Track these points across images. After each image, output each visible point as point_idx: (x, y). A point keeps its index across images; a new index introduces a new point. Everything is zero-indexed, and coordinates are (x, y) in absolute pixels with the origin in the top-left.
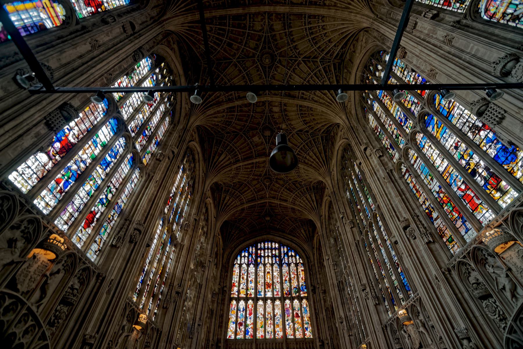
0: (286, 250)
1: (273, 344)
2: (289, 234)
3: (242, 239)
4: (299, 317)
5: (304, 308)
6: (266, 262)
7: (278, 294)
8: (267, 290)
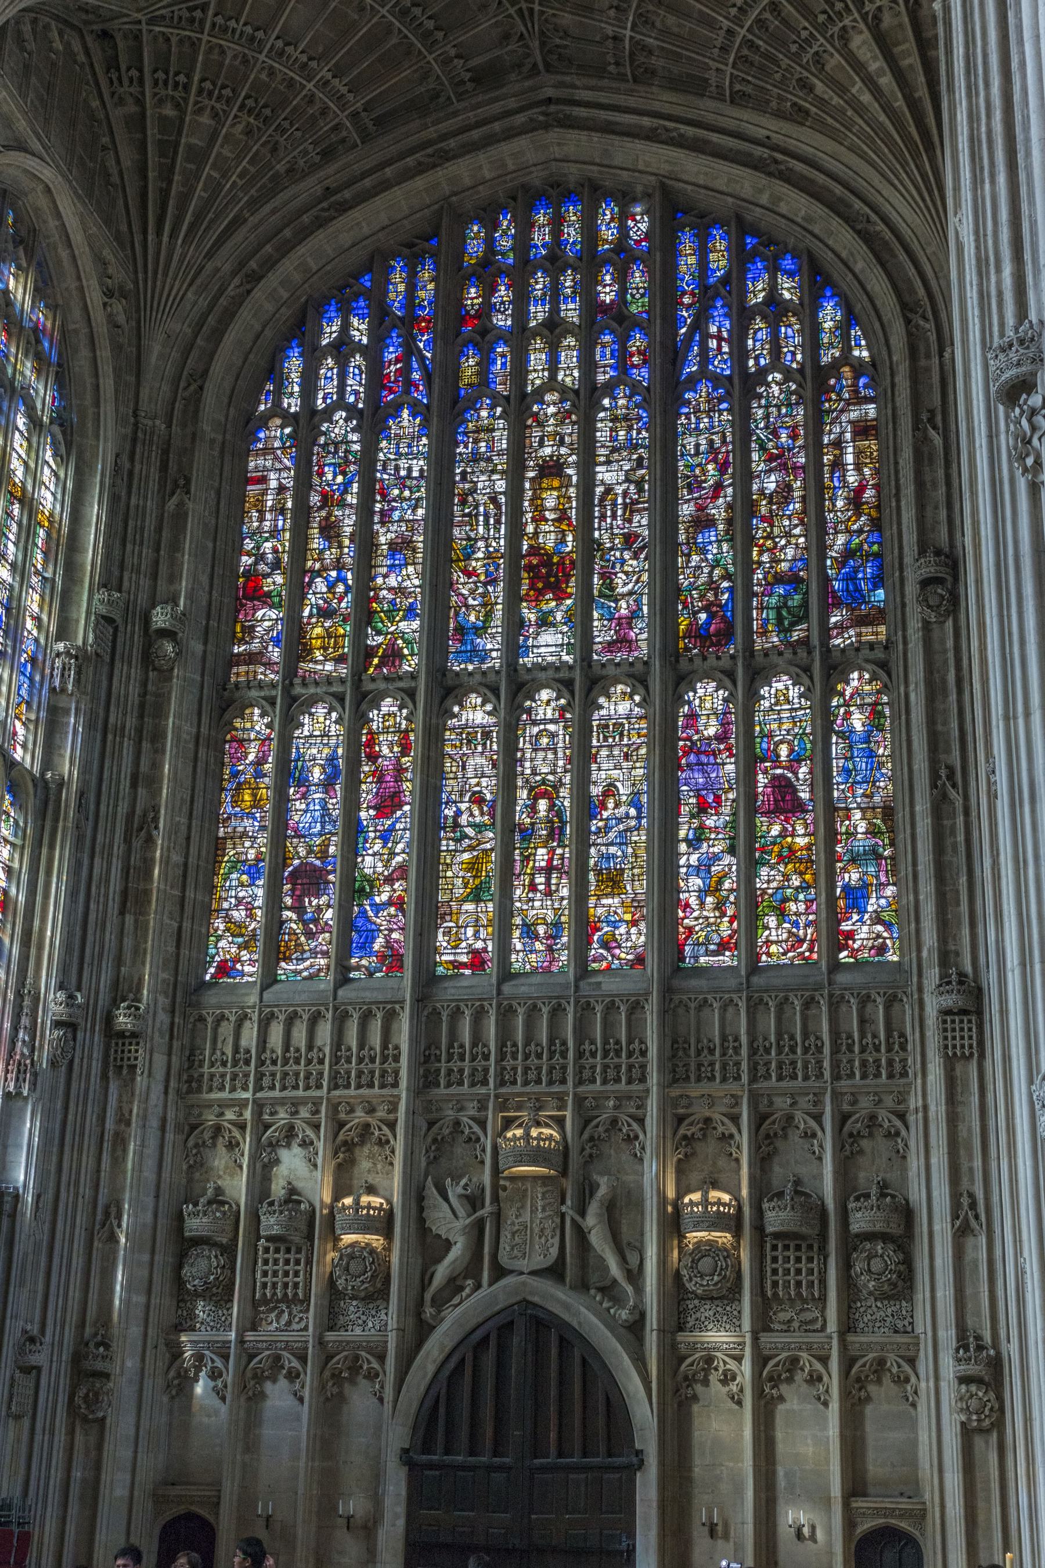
0: (719, 262)
1: (557, 1011)
2: (737, 99)
3: (308, 188)
4: (799, 807)
5: (846, 735)
6: (537, 377)
7: (622, 642)
8: (530, 615)
